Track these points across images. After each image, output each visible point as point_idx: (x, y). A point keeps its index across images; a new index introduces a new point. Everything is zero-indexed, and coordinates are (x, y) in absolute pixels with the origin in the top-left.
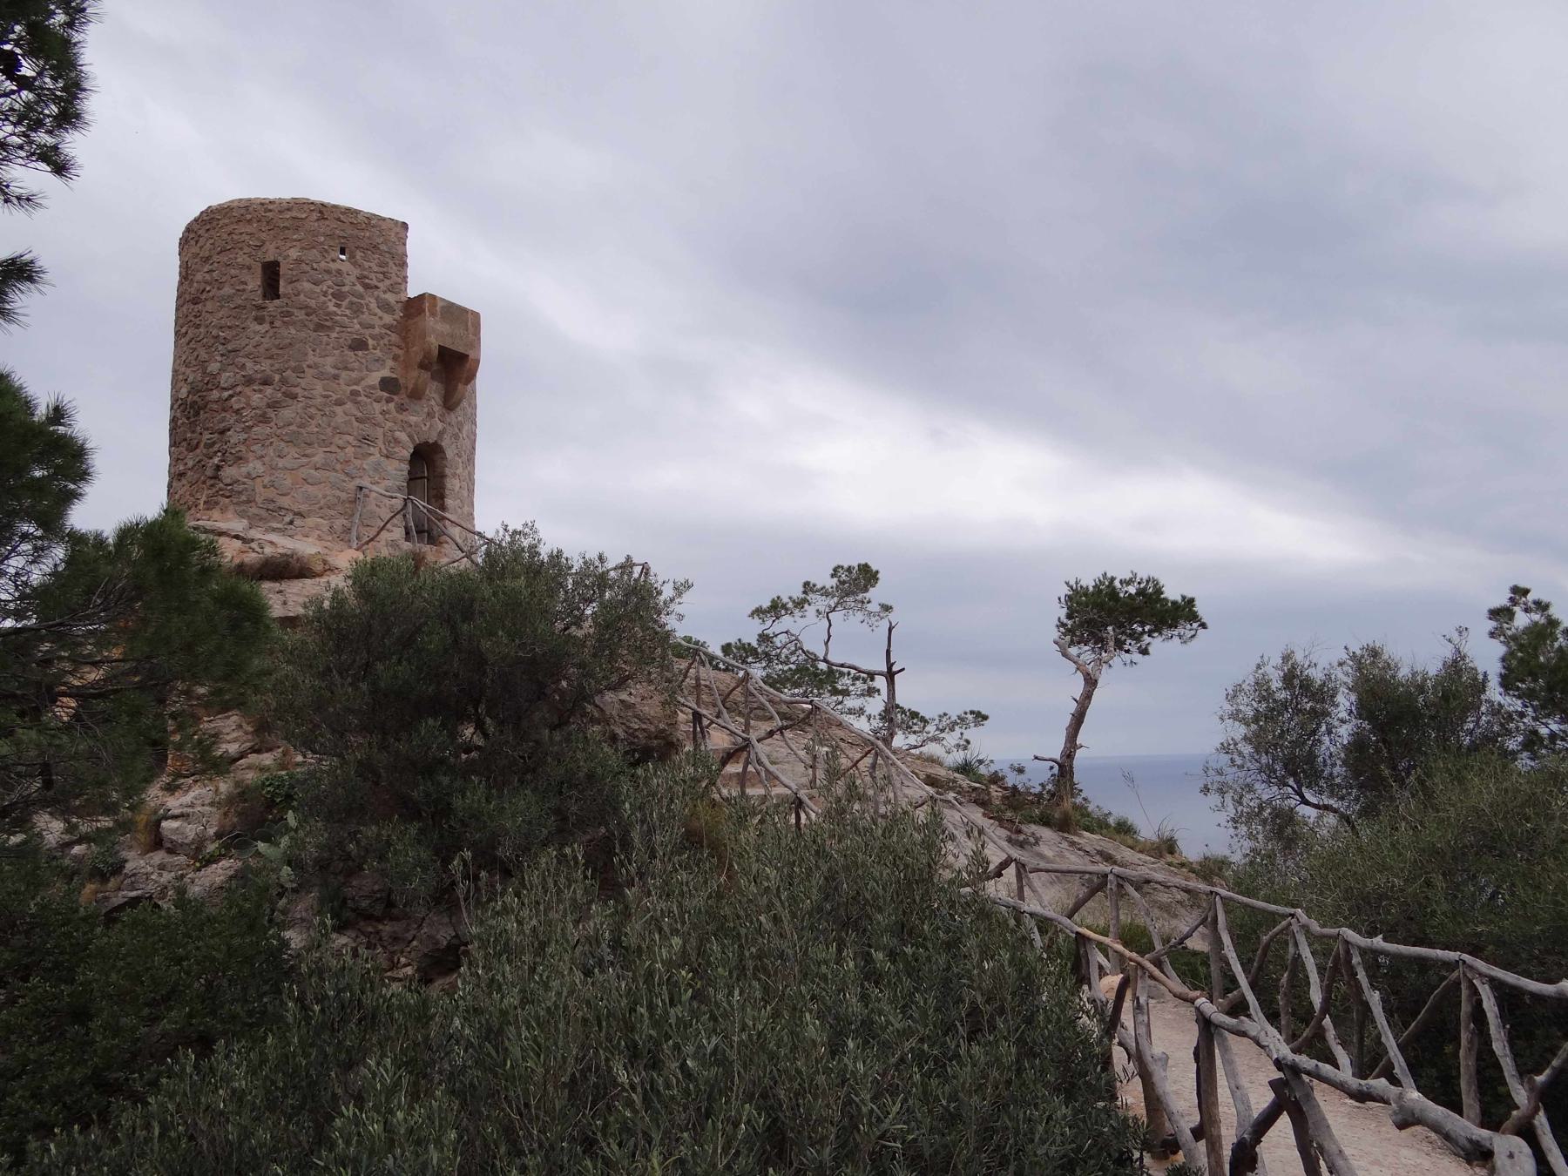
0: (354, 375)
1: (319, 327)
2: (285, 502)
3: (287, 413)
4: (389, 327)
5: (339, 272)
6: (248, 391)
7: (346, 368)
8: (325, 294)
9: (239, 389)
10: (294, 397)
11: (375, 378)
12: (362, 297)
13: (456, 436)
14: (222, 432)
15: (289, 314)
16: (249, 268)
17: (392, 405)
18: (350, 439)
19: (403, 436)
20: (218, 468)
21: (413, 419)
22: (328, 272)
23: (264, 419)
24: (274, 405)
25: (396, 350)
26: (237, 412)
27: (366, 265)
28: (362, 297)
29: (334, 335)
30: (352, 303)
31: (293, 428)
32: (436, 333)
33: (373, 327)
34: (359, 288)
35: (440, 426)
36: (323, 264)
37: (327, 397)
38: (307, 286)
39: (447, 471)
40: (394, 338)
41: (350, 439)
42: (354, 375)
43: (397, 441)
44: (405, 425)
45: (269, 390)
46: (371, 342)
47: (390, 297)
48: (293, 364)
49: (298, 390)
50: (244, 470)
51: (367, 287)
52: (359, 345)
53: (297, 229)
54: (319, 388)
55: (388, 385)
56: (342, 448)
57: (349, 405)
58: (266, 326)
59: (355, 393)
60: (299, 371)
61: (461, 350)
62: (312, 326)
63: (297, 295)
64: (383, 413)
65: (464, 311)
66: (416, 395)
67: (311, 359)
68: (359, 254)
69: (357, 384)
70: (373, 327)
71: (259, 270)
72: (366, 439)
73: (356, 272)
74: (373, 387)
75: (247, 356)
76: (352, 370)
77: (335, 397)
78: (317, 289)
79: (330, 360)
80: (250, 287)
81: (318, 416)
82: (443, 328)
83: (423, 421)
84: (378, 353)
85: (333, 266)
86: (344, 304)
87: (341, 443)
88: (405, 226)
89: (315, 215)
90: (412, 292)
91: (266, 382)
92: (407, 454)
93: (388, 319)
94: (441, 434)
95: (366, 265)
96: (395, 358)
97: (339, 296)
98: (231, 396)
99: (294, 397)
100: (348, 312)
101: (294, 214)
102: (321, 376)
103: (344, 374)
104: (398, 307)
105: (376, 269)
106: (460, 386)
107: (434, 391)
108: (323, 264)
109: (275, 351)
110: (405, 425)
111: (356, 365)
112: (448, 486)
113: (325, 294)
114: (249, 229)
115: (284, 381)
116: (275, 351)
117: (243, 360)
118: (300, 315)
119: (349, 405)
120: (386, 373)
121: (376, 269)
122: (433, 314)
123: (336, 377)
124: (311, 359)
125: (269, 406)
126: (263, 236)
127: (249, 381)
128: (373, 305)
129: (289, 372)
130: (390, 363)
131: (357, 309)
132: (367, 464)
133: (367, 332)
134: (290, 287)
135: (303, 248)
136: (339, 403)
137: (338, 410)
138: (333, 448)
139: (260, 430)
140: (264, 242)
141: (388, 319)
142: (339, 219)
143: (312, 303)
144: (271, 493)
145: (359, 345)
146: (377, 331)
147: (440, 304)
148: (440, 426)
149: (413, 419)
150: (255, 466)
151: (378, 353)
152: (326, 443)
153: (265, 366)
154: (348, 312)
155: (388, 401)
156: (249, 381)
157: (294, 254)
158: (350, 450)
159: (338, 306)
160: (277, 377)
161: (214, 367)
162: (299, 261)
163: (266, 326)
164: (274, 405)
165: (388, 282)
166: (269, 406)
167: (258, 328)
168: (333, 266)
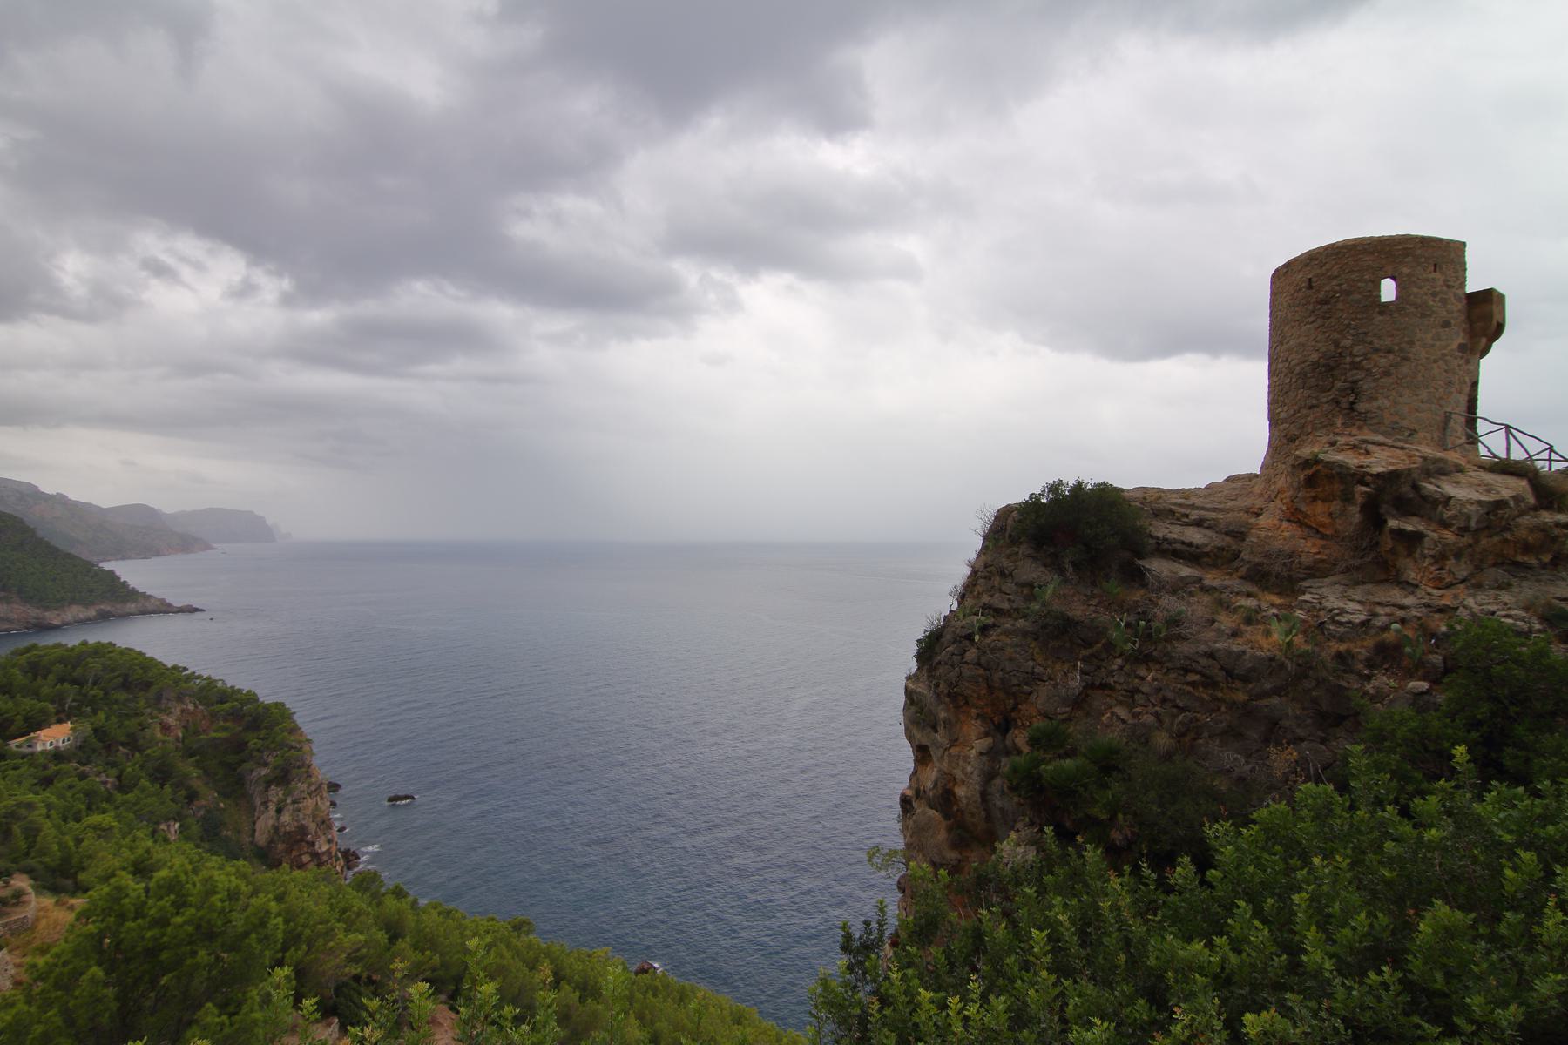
1: (1423, 315)
2: (1405, 423)
3: (1405, 369)
6: (1375, 357)
10: (1407, 359)
11: (1455, 345)
23: (1387, 374)
45: (1391, 356)
47: (1460, 292)
50: (1375, 404)
54: (1423, 354)
55: (1462, 348)
60: (1411, 343)
67: (1419, 335)
88: (1464, 244)
90: (1471, 287)
91: (1389, 351)
97: (1434, 295)
99: (1407, 359)
115: (1401, 350)
120: (1460, 341)
124: (1419, 335)
127: (1377, 350)
136: (1435, 361)
144: (1396, 418)
145: (1446, 324)
150: (1382, 402)
153: (1388, 341)
156: (1377, 350)
161: (1347, 343)
162: (1409, 275)
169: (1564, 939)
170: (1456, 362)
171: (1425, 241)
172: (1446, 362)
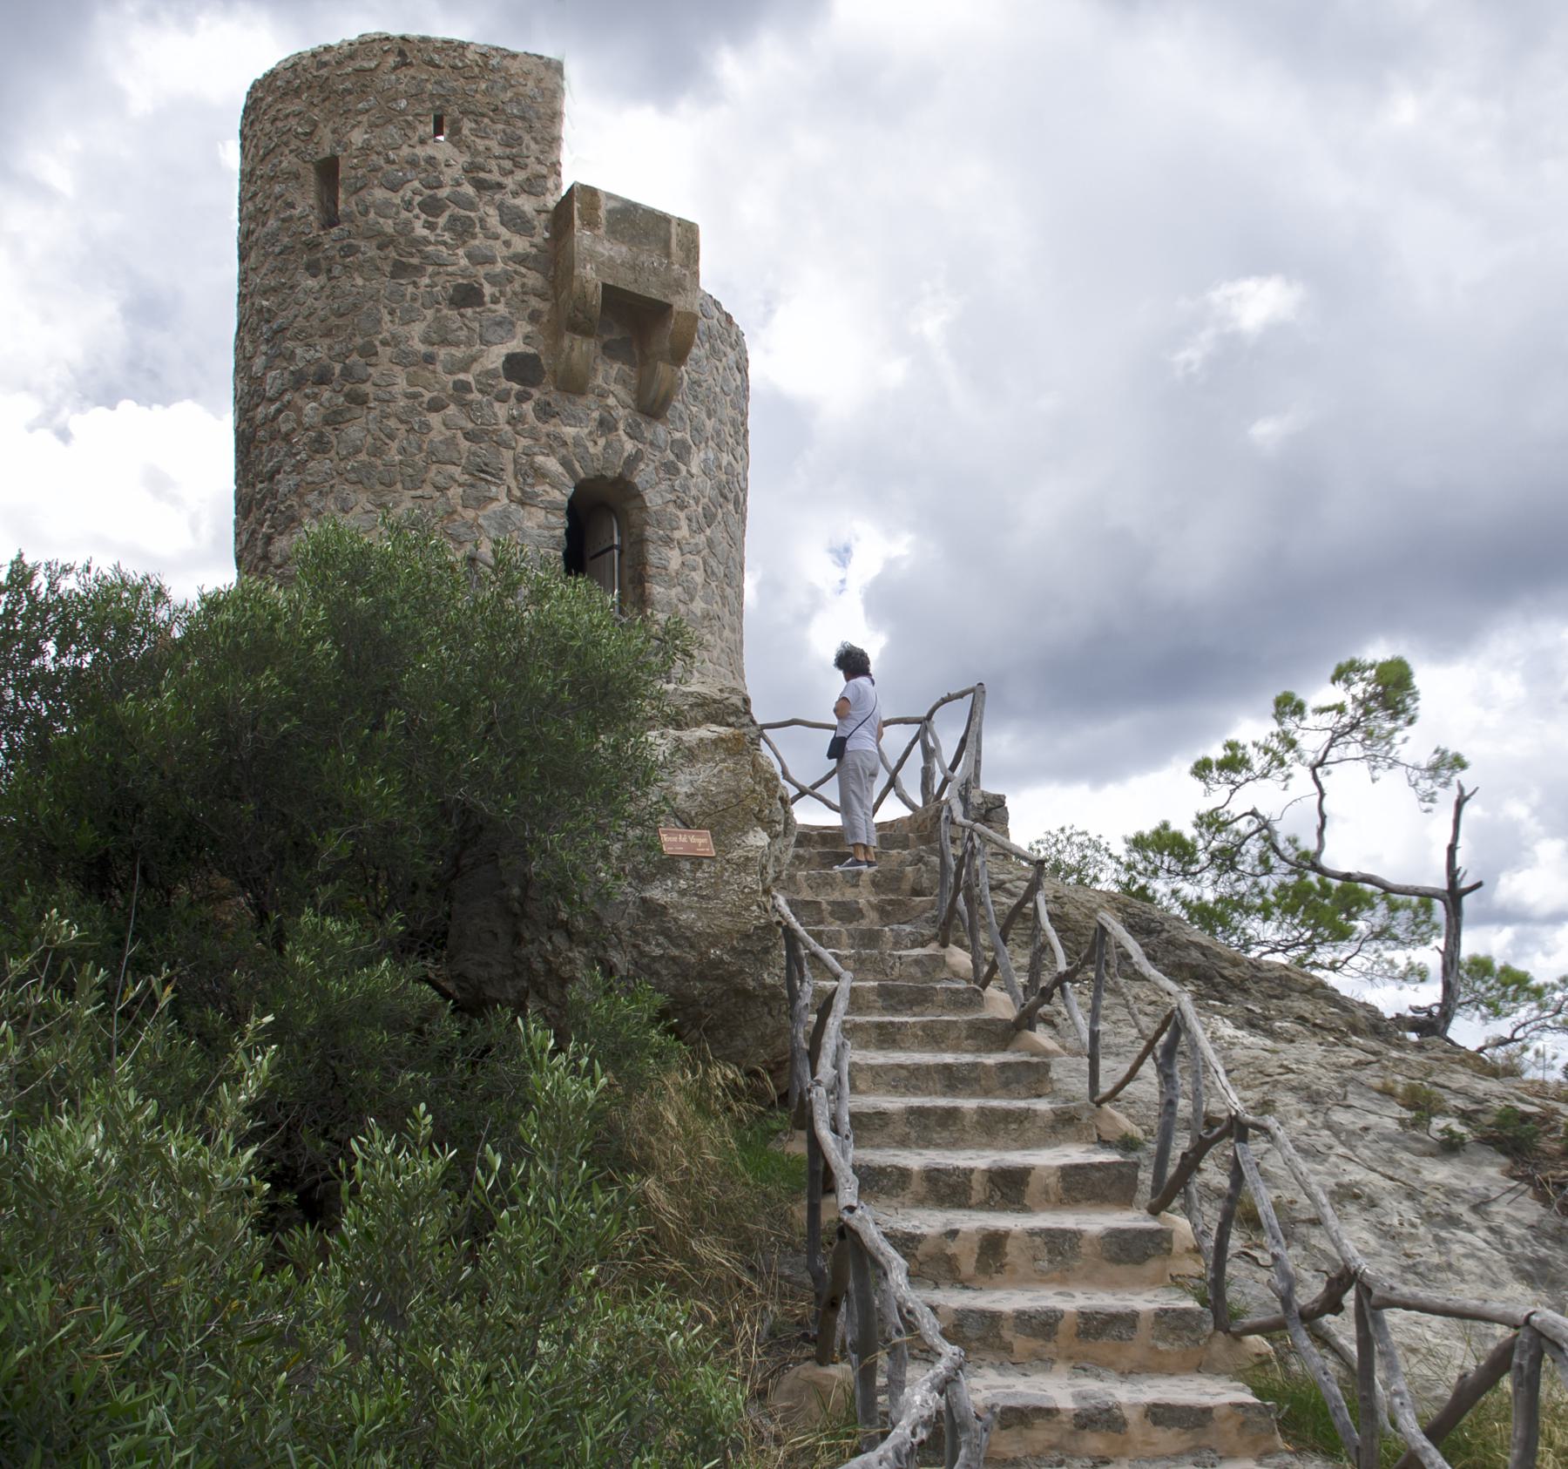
0: (459, 353)
1: (400, 270)
3: (354, 432)
4: (521, 259)
5: (431, 160)
7: (445, 342)
8: (408, 205)
9: (287, 397)
10: (359, 400)
11: (495, 357)
12: (471, 206)
13: (671, 469)
14: (271, 478)
15: (351, 250)
16: (297, 176)
17: (528, 407)
18: (456, 471)
19: (552, 464)
20: (269, 539)
21: (569, 431)
22: (413, 163)
23: (320, 445)
24: (334, 418)
25: (535, 303)
26: (287, 437)
27: (481, 144)
28: (471, 206)
29: (426, 281)
30: (453, 219)
31: (363, 457)
32: (598, 258)
33: (491, 260)
34: (468, 189)
35: (629, 446)
36: (405, 150)
37: (414, 396)
38: (380, 194)
39: (650, 532)
40: (534, 279)
41: (456, 471)
42: (459, 353)
43: (540, 474)
44: (555, 443)
46: (488, 290)
47: (526, 204)
48: (359, 341)
49: (367, 388)
51: (480, 185)
52: (467, 296)
53: (363, 92)
56: (442, 490)
57: (452, 409)
58: (323, 278)
59: (462, 387)
60: (368, 351)
61: (655, 293)
62: (388, 269)
63: (365, 213)
64: (512, 421)
65: (662, 220)
66: (574, 385)
68: (467, 126)
69: (466, 370)
70: (491, 260)
71: (312, 178)
72: (482, 472)
73: (464, 159)
74: (491, 374)
75: (295, 338)
76: (457, 344)
77: (427, 396)
78: (397, 199)
79: (418, 329)
80: (297, 212)
81: (402, 433)
82: (608, 249)
83: (587, 434)
84: (501, 308)
85: (421, 152)
86: (442, 221)
87: (440, 480)
89: (392, 60)
91: (323, 378)
92: (561, 497)
93: (521, 244)
94: (637, 457)
95: (481, 144)
96: (534, 317)
97: (432, 207)
98: (279, 411)
99: (359, 400)
100: (447, 237)
101: (358, 64)
102: (404, 359)
103: (442, 353)
104: (540, 222)
105: (498, 150)
106: (663, 368)
107: (611, 382)
108: (405, 150)
109: (333, 321)
110: (555, 443)
111: (463, 334)
112: (653, 558)
113: (408, 205)
114: (296, 106)
115: (347, 373)
116: (333, 321)
117: (290, 344)
118: (369, 249)
119: (452, 409)
120: (516, 345)
121: (498, 150)
122: (591, 223)
123: (430, 359)
124: (388, 327)
125: (327, 422)
126: (316, 114)
128: (494, 221)
129: (355, 357)
130: (524, 327)
131: (462, 229)
132: (484, 516)
133: (481, 271)
134: (353, 200)
135: (372, 125)
136: (436, 406)
137: (435, 419)
138: (427, 490)
139: (320, 466)
140: (315, 124)
141: (521, 244)
142: (431, 63)
143: (388, 226)
145: (467, 296)
146: (499, 266)
147: (605, 206)
148: (629, 446)
149: (569, 431)
151: (501, 308)
152: (416, 482)
153: (321, 351)
154: (447, 237)
155: (522, 398)
156: (299, 380)
157: (357, 137)
158: (455, 492)
159: (431, 226)
160: (338, 368)
162: (366, 149)
163: (323, 278)
164: (334, 418)
165: (520, 175)
166: (327, 422)
167: (311, 283)
168: (421, 152)
169: (1501, 1467)
170: (501, 411)
171: (404, 50)
172: (464, 405)
